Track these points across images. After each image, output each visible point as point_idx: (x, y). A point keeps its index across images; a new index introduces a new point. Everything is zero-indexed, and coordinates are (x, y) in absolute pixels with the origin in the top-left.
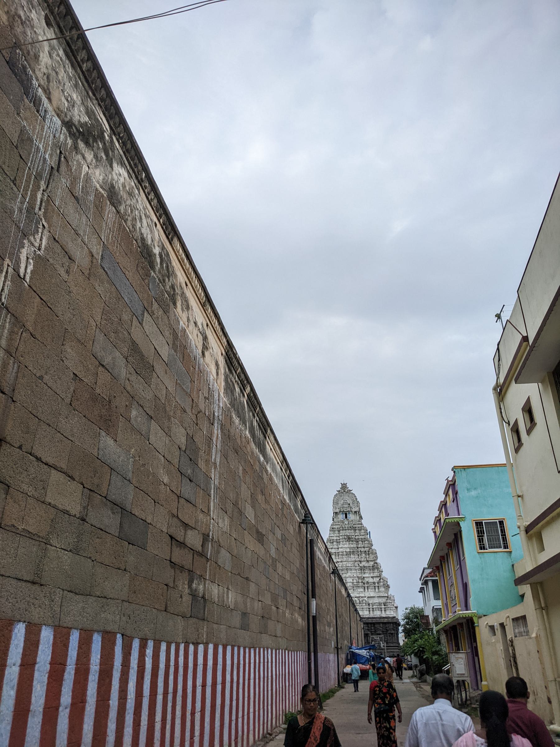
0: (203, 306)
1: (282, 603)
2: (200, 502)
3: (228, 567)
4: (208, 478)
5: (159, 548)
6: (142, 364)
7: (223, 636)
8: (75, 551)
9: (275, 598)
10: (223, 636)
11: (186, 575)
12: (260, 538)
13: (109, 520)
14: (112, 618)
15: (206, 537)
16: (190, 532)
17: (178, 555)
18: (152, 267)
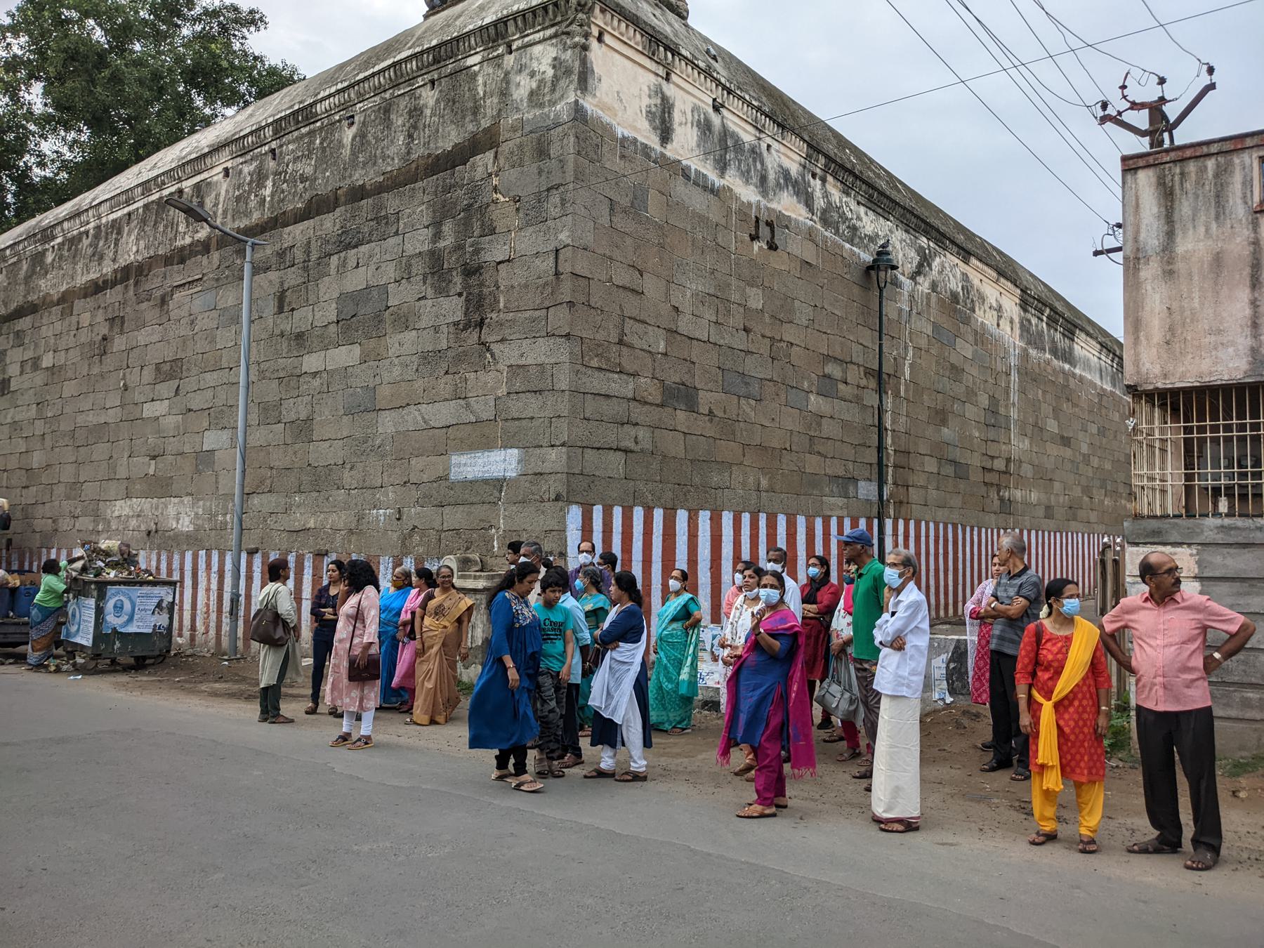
0: (997, 282)
1: (1098, 495)
3: (1030, 475)
4: (1007, 417)
5: (976, 476)
6: (956, 372)
7: (1027, 524)
8: (938, 489)
9: (1087, 490)
12: (1066, 441)
13: (949, 470)
14: (955, 517)
15: (1008, 460)
16: (996, 461)
17: (989, 477)
18: (958, 303)
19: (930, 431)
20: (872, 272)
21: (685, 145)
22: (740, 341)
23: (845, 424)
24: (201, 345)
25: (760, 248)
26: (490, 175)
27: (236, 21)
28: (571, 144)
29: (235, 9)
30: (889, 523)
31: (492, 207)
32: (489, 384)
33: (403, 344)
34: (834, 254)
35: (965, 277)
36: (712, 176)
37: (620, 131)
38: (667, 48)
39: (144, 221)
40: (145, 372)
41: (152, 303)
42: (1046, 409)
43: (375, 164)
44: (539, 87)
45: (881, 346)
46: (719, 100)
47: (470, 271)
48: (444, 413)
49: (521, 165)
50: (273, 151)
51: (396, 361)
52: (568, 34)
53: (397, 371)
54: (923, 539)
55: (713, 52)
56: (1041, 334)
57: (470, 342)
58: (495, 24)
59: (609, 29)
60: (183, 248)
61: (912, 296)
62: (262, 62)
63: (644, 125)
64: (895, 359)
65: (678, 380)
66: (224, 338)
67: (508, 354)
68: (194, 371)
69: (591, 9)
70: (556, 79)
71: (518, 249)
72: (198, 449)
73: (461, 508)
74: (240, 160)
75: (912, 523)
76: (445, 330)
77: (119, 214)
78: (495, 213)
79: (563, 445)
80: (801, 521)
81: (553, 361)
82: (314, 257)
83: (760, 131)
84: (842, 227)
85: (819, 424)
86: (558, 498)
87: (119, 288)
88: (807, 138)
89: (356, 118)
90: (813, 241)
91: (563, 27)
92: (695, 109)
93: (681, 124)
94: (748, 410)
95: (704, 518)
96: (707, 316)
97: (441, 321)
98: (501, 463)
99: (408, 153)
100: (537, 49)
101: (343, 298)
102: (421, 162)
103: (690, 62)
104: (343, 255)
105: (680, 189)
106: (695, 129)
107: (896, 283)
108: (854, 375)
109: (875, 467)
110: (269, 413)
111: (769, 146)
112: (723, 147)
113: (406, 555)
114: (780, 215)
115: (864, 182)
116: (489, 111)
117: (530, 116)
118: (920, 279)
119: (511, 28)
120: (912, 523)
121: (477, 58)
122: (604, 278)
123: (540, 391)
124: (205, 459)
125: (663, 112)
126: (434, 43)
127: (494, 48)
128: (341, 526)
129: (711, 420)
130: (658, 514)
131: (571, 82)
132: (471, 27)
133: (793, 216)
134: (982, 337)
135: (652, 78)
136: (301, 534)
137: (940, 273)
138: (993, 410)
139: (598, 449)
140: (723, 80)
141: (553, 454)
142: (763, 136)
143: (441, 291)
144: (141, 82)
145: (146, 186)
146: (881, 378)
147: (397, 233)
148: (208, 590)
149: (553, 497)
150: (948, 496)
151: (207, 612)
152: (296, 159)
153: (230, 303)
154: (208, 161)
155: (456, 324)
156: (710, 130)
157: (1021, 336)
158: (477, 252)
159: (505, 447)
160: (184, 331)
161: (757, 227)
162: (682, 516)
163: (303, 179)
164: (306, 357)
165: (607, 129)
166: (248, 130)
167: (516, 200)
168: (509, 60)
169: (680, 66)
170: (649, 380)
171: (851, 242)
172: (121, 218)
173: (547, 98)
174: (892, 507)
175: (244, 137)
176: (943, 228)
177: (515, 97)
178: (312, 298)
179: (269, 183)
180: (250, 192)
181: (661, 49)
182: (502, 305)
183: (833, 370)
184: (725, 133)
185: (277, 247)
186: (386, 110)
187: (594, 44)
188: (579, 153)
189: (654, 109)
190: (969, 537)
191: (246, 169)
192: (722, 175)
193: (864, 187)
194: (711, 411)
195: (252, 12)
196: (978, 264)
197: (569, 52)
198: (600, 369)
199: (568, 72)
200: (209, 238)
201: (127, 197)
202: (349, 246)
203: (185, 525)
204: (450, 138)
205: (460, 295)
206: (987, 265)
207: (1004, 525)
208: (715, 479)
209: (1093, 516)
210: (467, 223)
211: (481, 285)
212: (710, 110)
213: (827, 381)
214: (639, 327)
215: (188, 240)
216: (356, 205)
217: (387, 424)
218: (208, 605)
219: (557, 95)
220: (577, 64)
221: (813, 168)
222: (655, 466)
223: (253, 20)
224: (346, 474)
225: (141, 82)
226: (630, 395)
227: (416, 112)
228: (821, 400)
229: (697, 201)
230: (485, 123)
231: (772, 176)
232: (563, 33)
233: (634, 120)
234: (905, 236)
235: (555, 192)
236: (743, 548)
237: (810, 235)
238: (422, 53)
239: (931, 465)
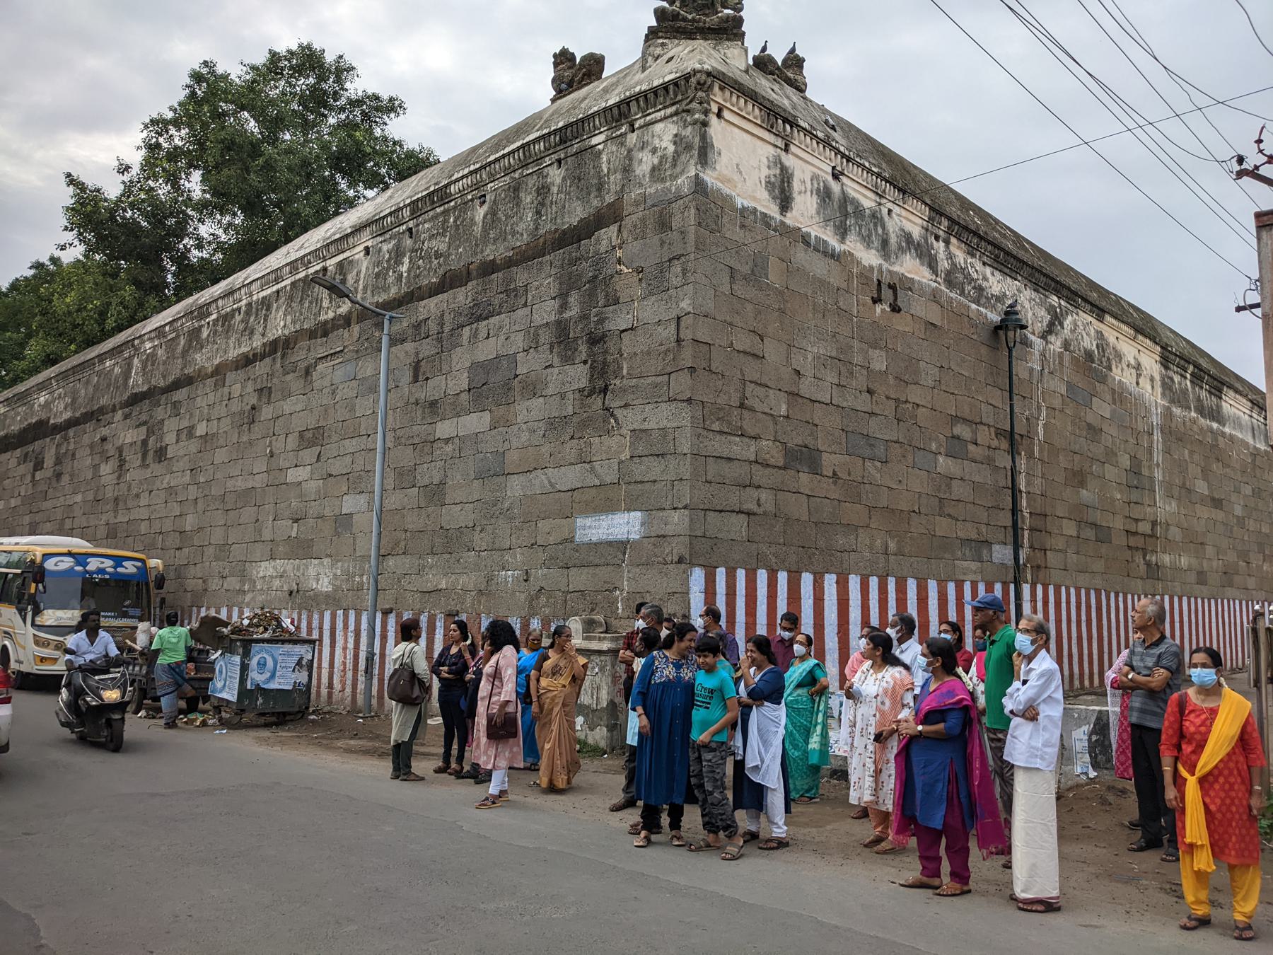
0: (1134, 339)
1: (1256, 559)
2: (1147, 501)
4: (1152, 478)
6: (1094, 432)
7: (1178, 589)
8: (1078, 553)
9: (1244, 555)
10: (1178, 589)
11: (1140, 553)
12: (1217, 503)
13: (1089, 533)
14: (1098, 582)
15: (1154, 523)
17: (1133, 541)
18: (1093, 362)
19: (1068, 493)
20: (1001, 333)
21: (805, 213)
22: (863, 403)
23: (976, 486)
24: (342, 414)
25: (883, 311)
26: (614, 247)
27: (377, 109)
28: (692, 217)
29: (376, 98)
30: (1026, 588)
31: (616, 278)
32: (612, 449)
33: (530, 411)
34: (960, 315)
35: (1100, 335)
36: (833, 242)
37: (740, 202)
38: (785, 120)
39: (291, 298)
40: (290, 438)
41: (296, 374)
42: (1194, 470)
43: (505, 240)
44: (660, 163)
45: (1011, 406)
46: (839, 168)
47: (595, 340)
48: (570, 476)
49: (644, 238)
50: (410, 230)
51: (524, 427)
52: (688, 111)
53: (525, 436)
54: (1064, 605)
55: (831, 122)
56: (1184, 392)
57: (594, 407)
58: (618, 105)
59: (728, 105)
60: (326, 322)
61: (1043, 355)
62: (401, 146)
63: (764, 195)
64: (1028, 419)
65: (800, 443)
66: (363, 406)
67: (630, 419)
68: (335, 438)
69: (711, 87)
70: (677, 154)
71: (641, 317)
72: (337, 512)
73: (586, 570)
74: (380, 239)
75: (1051, 589)
76: (571, 397)
77: (269, 291)
78: (619, 284)
79: (685, 508)
80: (932, 586)
81: (674, 425)
82: (447, 329)
83: (881, 196)
84: (968, 288)
85: (949, 486)
86: (680, 561)
87: (267, 360)
88: (928, 202)
89: (488, 197)
90: (938, 302)
91: (683, 106)
92: (814, 177)
93: (800, 193)
94: (873, 472)
95: (830, 581)
96: (829, 379)
97: (567, 388)
98: (624, 525)
99: (537, 229)
100: (658, 127)
101: (474, 367)
102: (548, 236)
103: (809, 133)
104: (474, 326)
105: (801, 256)
106: (815, 197)
107: (1026, 343)
108: (984, 435)
109: (1010, 530)
110: (404, 477)
111: (890, 211)
112: (843, 213)
113: (533, 616)
114: (903, 278)
115: (989, 243)
116: (613, 187)
117: (652, 190)
118: (1052, 338)
119: (634, 108)
120: (1051, 589)
121: (601, 138)
122: (724, 344)
123: (663, 455)
124: (343, 522)
125: (783, 181)
126: (561, 124)
127: (618, 128)
128: (471, 587)
129: (835, 483)
130: (782, 577)
131: (691, 157)
132: (596, 109)
133: (917, 278)
134: (1120, 396)
135: (771, 150)
136: (433, 595)
137: (1073, 331)
138: (1135, 470)
139: (721, 511)
140: (842, 149)
141: (676, 516)
142: (884, 201)
143: (567, 359)
144: (290, 168)
145: (293, 266)
146: (1013, 439)
147: (525, 305)
148: (345, 649)
149: (676, 559)
150: (1089, 559)
151: (344, 670)
152: (431, 237)
153: (368, 374)
154: (351, 240)
155: (581, 390)
156: (829, 197)
157: (1163, 394)
158: (601, 321)
159: (629, 510)
160: (326, 400)
161: (879, 290)
162: (807, 580)
163: (438, 255)
164: (439, 424)
165: (728, 200)
166: (388, 211)
167: (639, 270)
168: (632, 138)
169: (798, 137)
170: (770, 443)
171: (978, 303)
172: (270, 296)
173: (668, 173)
174: (1029, 571)
175: (383, 218)
176: (1074, 287)
177: (637, 172)
178: (445, 368)
179: (406, 260)
180: (388, 269)
181: (780, 121)
182: (625, 372)
183: (962, 431)
184: (845, 199)
185: (413, 320)
186: (515, 189)
187: (713, 120)
188: (699, 224)
189: (773, 179)
190: (1113, 603)
191: (385, 247)
192: (843, 240)
193: (989, 247)
194: (835, 474)
195: (391, 100)
196: (1113, 321)
197: (690, 129)
198: (721, 432)
199: (689, 147)
200: (350, 312)
201: (276, 276)
202: (480, 318)
203: (325, 585)
204: (577, 213)
205: (585, 362)
206: (1123, 322)
207: (1152, 591)
208: (841, 541)
209: (1251, 582)
210: (592, 294)
211: (606, 352)
212: (830, 178)
213: (956, 441)
214: (761, 391)
215: (331, 315)
216: (485, 279)
217: (516, 487)
218: (344, 664)
219: (678, 169)
220: (697, 139)
221: (936, 231)
222: (778, 527)
223: (393, 107)
224: (477, 537)
225: (290, 168)
226: (752, 458)
227: (543, 190)
228: (950, 461)
229: (818, 267)
230: (609, 199)
231: (893, 240)
232: (684, 111)
233: (754, 191)
234: (1034, 295)
235: (676, 262)
236: (872, 613)
237: (935, 296)
238: (549, 134)
239: (1070, 529)
